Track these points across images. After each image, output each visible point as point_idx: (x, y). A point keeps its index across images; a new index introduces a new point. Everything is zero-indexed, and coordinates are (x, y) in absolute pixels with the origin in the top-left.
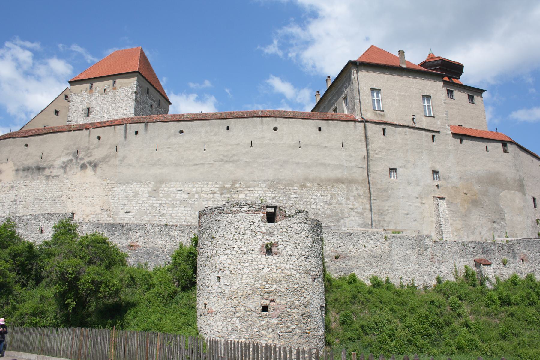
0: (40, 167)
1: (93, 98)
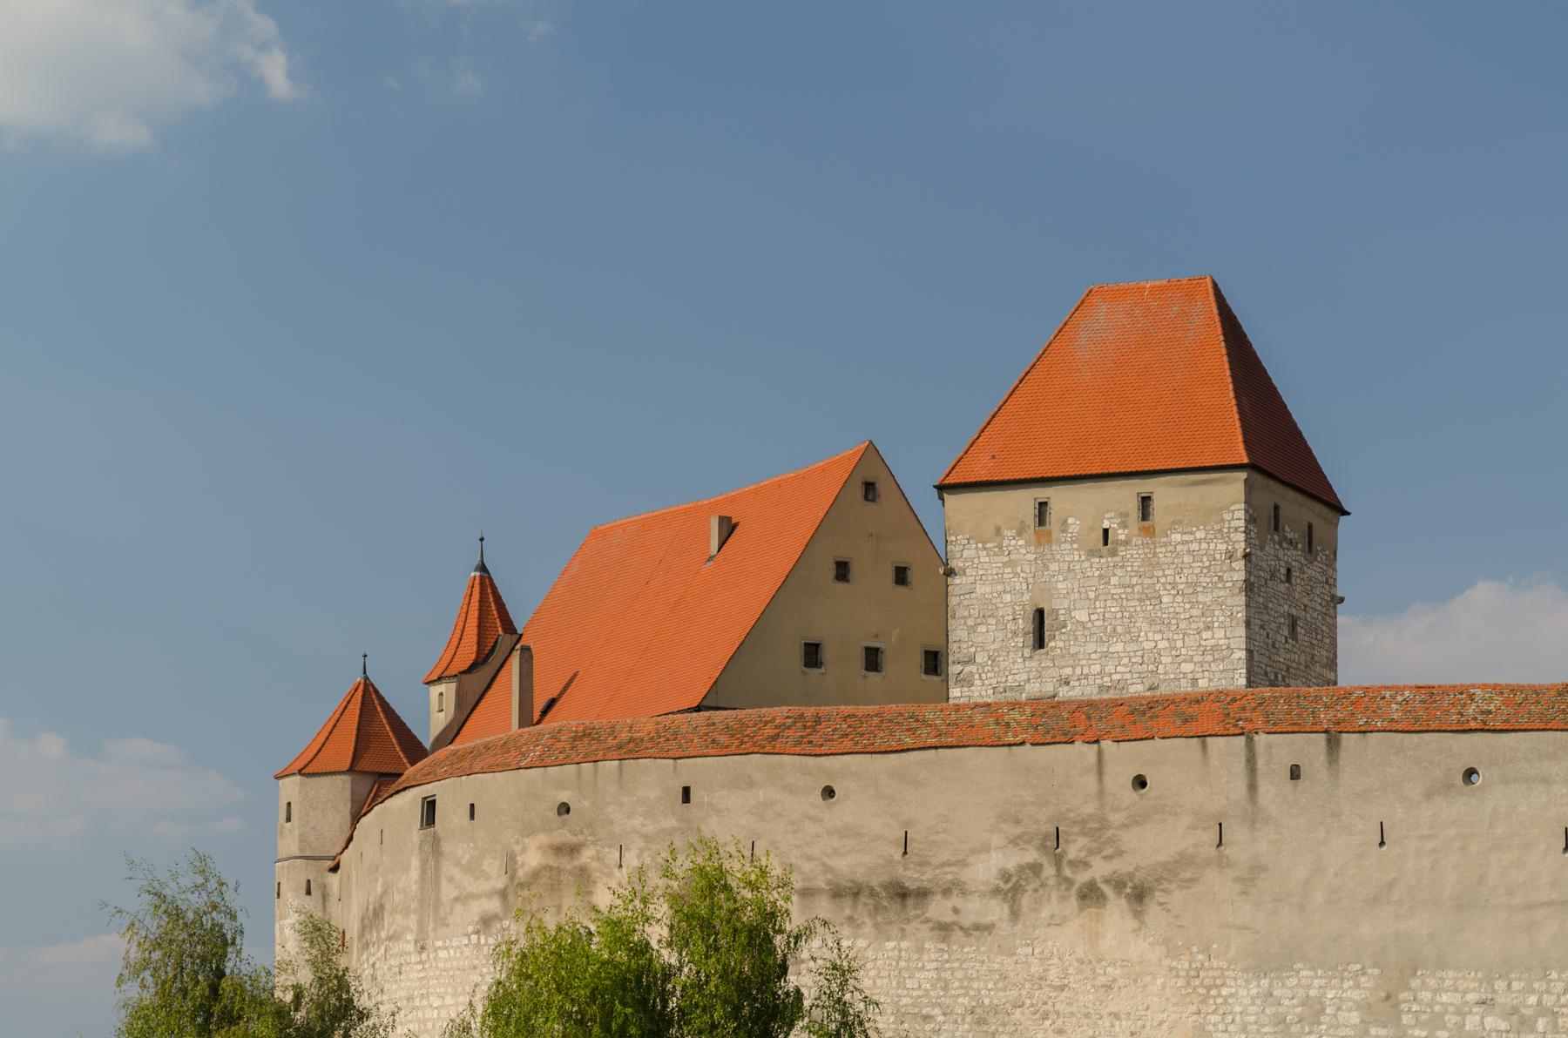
0: (903, 888)
1: (1054, 567)
